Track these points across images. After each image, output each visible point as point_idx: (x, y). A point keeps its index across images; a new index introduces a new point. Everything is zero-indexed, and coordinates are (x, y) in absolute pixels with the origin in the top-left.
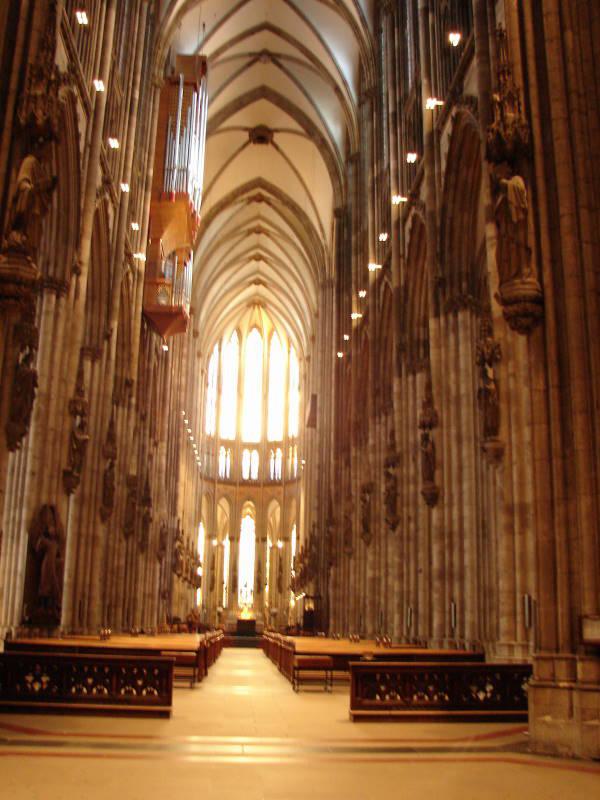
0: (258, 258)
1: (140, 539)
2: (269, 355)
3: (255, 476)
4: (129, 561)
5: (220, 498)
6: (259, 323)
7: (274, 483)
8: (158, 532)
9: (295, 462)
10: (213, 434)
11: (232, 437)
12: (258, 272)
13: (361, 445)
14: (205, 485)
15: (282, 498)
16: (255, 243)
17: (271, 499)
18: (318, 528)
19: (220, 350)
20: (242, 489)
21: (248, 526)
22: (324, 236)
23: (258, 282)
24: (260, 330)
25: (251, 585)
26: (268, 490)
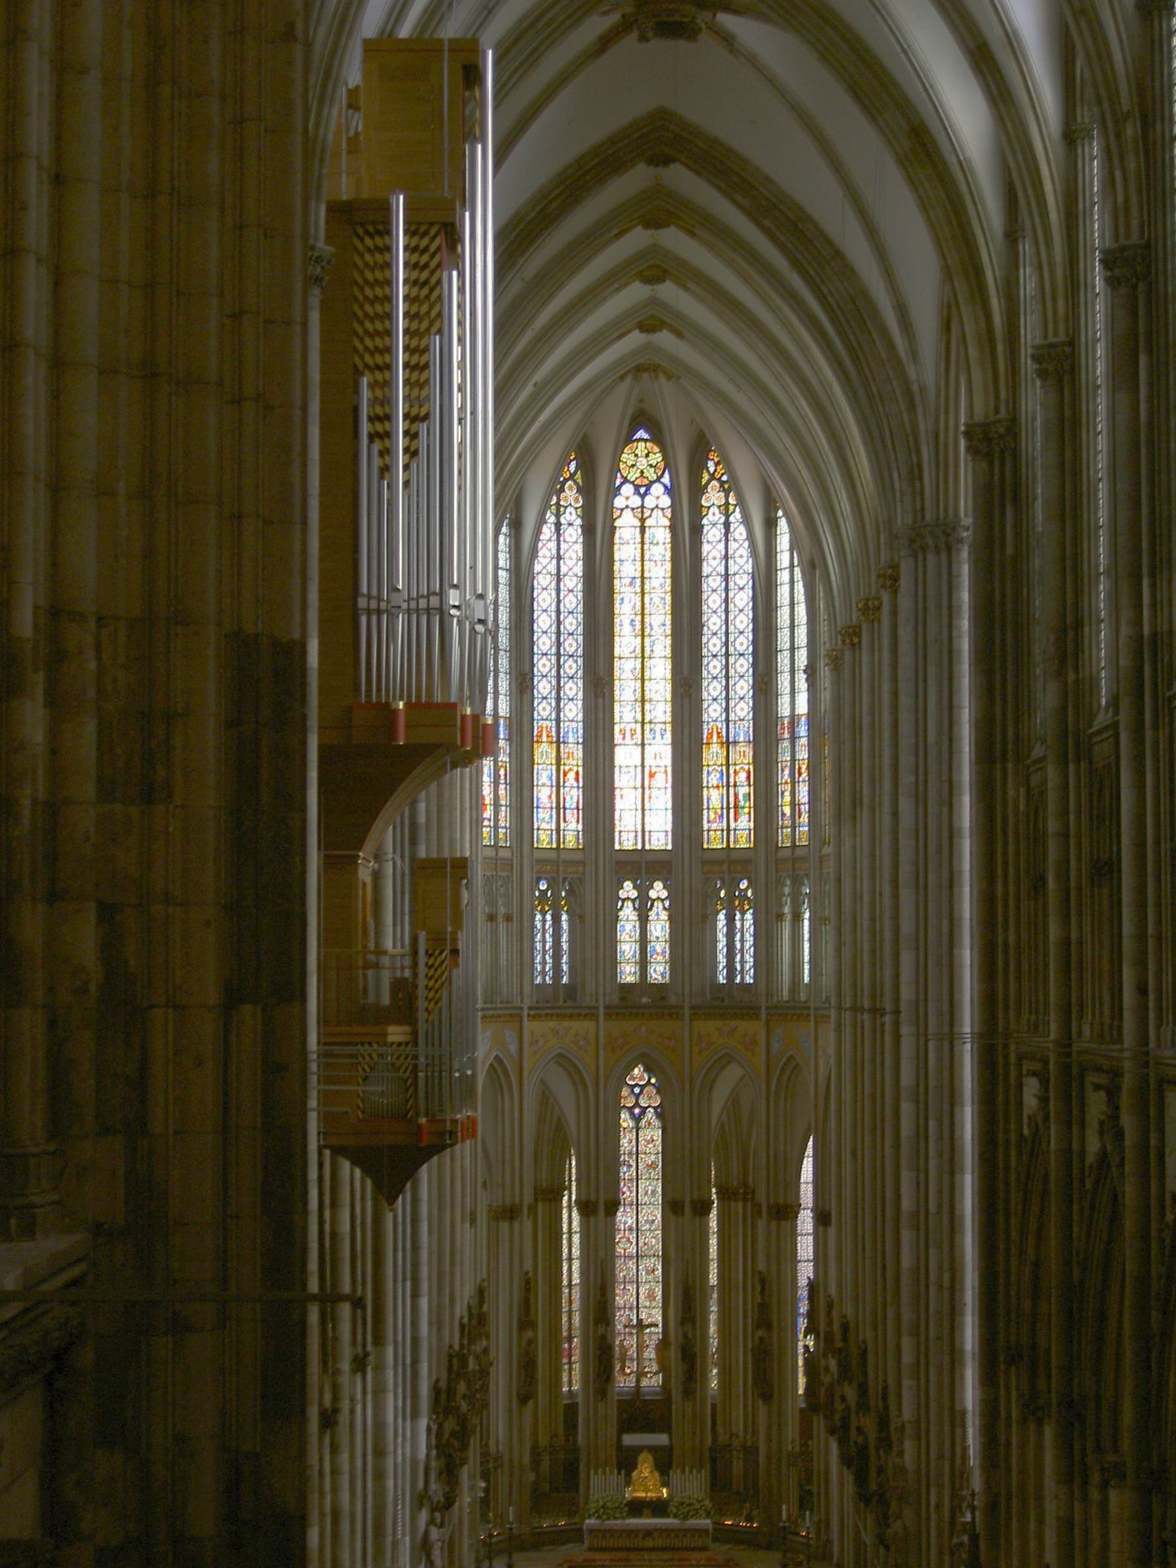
2: (697, 530)
9: (804, 946)
12: (653, 301)
17: (726, 1059)
26: (708, 1027)
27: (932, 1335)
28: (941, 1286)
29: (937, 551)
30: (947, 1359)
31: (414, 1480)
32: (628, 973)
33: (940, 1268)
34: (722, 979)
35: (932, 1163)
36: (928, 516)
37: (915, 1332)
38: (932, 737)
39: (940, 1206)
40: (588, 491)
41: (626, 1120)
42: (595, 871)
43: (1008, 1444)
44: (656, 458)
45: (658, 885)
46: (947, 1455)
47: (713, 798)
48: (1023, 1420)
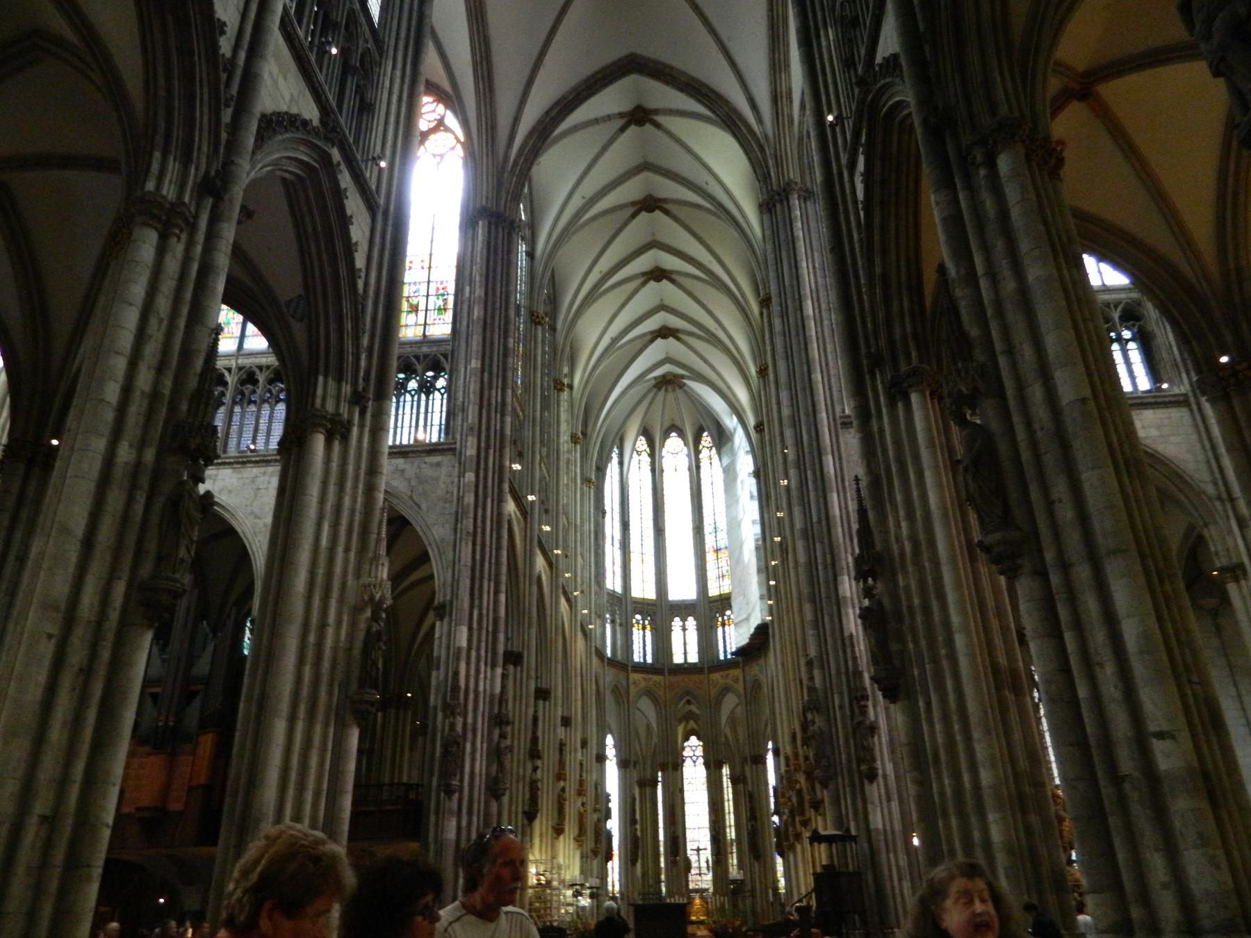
0: (658, 274)
1: (146, 570)
2: (698, 467)
3: (693, 658)
4: (76, 657)
5: (639, 697)
6: (678, 423)
7: (727, 665)
8: (361, 635)
10: (619, 589)
11: (651, 594)
13: (968, 178)
14: (610, 676)
15: (742, 691)
16: (649, 239)
17: (726, 690)
18: (822, 667)
19: (621, 463)
20: (674, 679)
21: (693, 748)
22: (760, 120)
23: (665, 332)
24: (682, 435)
25: (707, 855)
26: (716, 676)
27: (823, 595)
28: (825, 567)
29: (781, 201)
30: (835, 607)
31: (491, 709)
32: (678, 659)
33: (824, 554)
34: (722, 657)
35: (812, 494)
36: (775, 188)
37: (813, 600)
38: (787, 282)
39: (820, 519)
40: (652, 455)
41: (688, 764)
42: (660, 613)
43: (881, 431)
44: (680, 442)
45: (691, 619)
46: (843, 670)
47: (712, 574)
48: (892, 405)
